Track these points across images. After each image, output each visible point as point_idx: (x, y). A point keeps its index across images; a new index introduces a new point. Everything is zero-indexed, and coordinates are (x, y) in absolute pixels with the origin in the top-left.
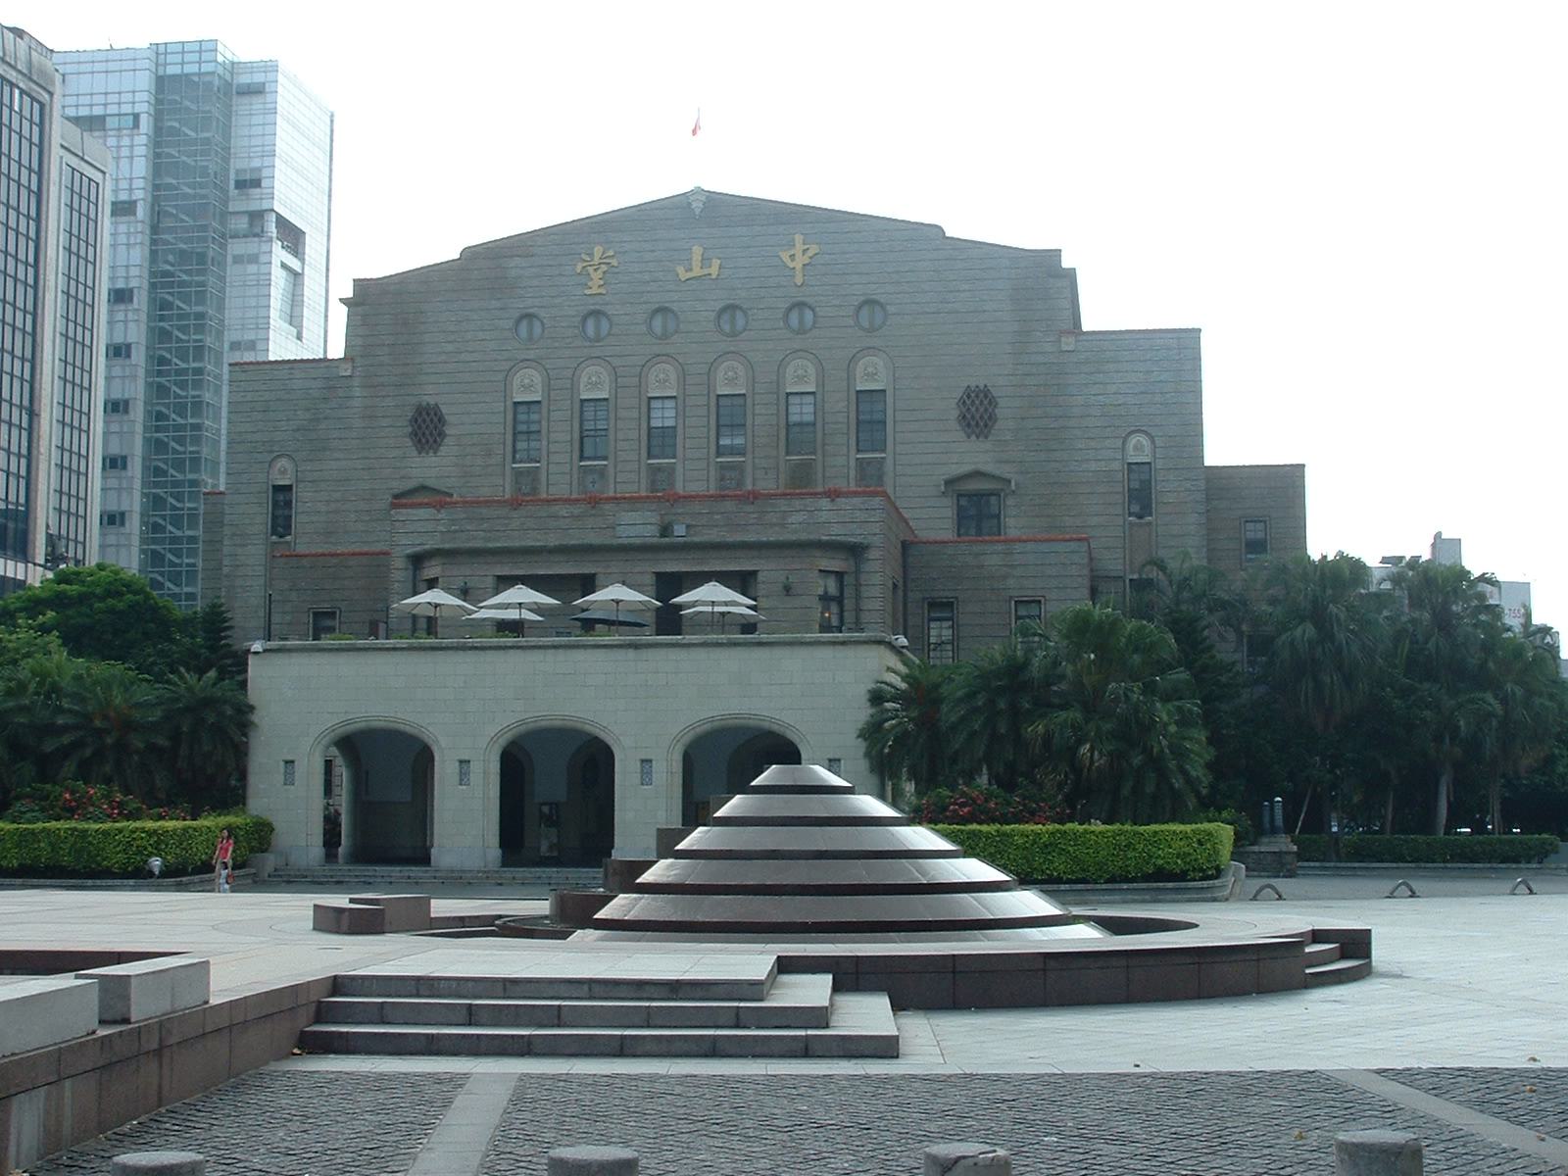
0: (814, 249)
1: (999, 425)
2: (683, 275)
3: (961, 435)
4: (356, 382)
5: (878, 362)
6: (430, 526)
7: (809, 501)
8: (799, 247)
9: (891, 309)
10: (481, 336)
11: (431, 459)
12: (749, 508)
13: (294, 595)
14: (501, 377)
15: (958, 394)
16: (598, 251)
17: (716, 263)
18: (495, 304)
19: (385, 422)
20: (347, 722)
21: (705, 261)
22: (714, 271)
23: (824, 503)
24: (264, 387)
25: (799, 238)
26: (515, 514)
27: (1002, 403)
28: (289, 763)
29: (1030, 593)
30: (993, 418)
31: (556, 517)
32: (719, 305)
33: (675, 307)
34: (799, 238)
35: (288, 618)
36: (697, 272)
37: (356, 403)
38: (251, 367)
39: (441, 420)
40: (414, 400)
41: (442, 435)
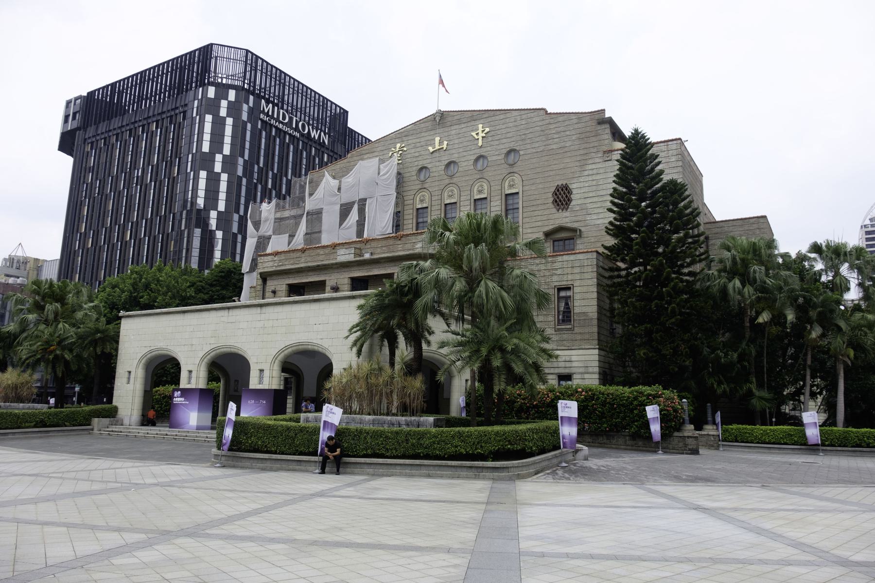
0: (487, 130)
1: (573, 203)
2: (431, 149)
3: (554, 210)
5: (517, 178)
6: (271, 264)
8: (481, 129)
9: (522, 153)
12: (399, 242)
15: (553, 189)
16: (398, 145)
17: (445, 143)
20: (151, 352)
21: (441, 143)
22: (445, 146)
25: (480, 126)
27: (574, 192)
28: (130, 372)
29: (564, 283)
30: (570, 200)
31: (318, 255)
32: (446, 162)
33: (429, 166)
34: (480, 126)
36: (437, 147)
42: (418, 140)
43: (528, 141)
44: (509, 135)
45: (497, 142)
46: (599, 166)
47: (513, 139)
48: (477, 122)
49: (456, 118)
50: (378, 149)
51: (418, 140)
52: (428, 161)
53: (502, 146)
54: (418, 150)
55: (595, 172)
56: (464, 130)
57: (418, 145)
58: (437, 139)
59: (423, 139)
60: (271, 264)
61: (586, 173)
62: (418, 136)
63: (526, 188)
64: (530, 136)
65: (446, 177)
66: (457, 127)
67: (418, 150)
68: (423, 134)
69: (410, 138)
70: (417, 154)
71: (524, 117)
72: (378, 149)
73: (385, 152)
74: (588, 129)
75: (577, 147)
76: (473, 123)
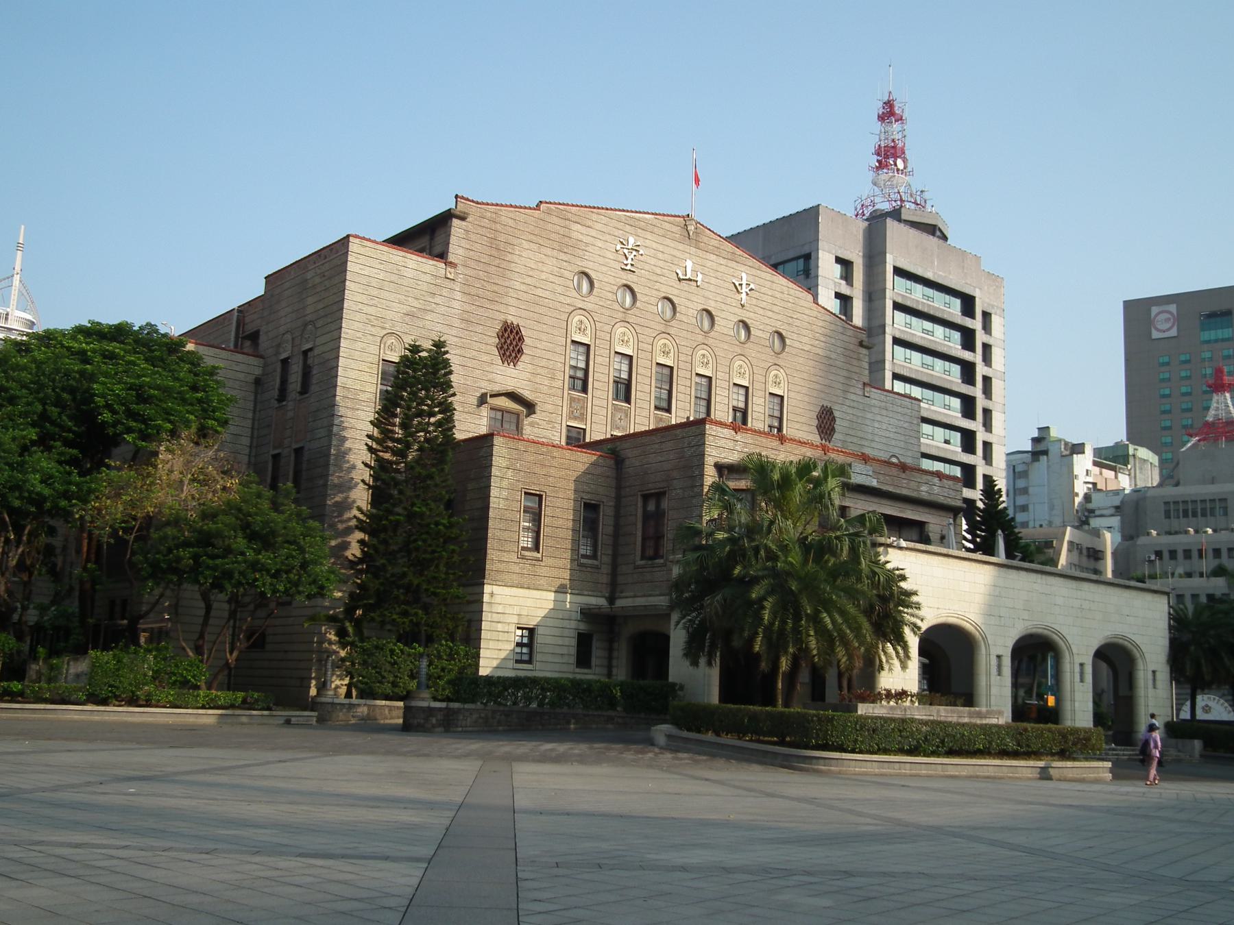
4: (457, 287)
7: (929, 478)
8: (744, 282)
10: (552, 278)
11: (509, 370)
12: (903, 476)
13: (510, 473)
14: (564, 317)
18: (562, 256)
19: (479, 329)
23: (936, 480)
24: (381, 267)
26: (782, 448)
35: (505, 493)
37: (456, 304)
38: (369, 244)
39: (521, 339)
40: (502, 317)
41: (520, 351)
42: (661, 248)
43: (795, 329)
44: (775, 309)
45: (761, 312)
46: (860, 399)
47: (779, 317)
48: (743, 268)
49: (714, 243)
50: (599, 226)
51: (661, 248)
52: (676, 292)
53: (767, 321)
54: (661, 263)
55: (855, 404)
56: (722, 269)
57: (660, 255)
58: (689, 264)
59: (667, 250)
60: (731, 444)
61: (848, 402)
62: (661, 240)
63: (792, 394)
64: (797, 323)
65: (698, 331)
66: (713, 257)
67: (661, 263)
68: (668, 242)
69: (649, 235)
70: (658, 271)
71: (792, 292)
72: (599, 226)
73: (608, 237)
74: (852, 347)
75: (839, 364)
76: (733, 264)
